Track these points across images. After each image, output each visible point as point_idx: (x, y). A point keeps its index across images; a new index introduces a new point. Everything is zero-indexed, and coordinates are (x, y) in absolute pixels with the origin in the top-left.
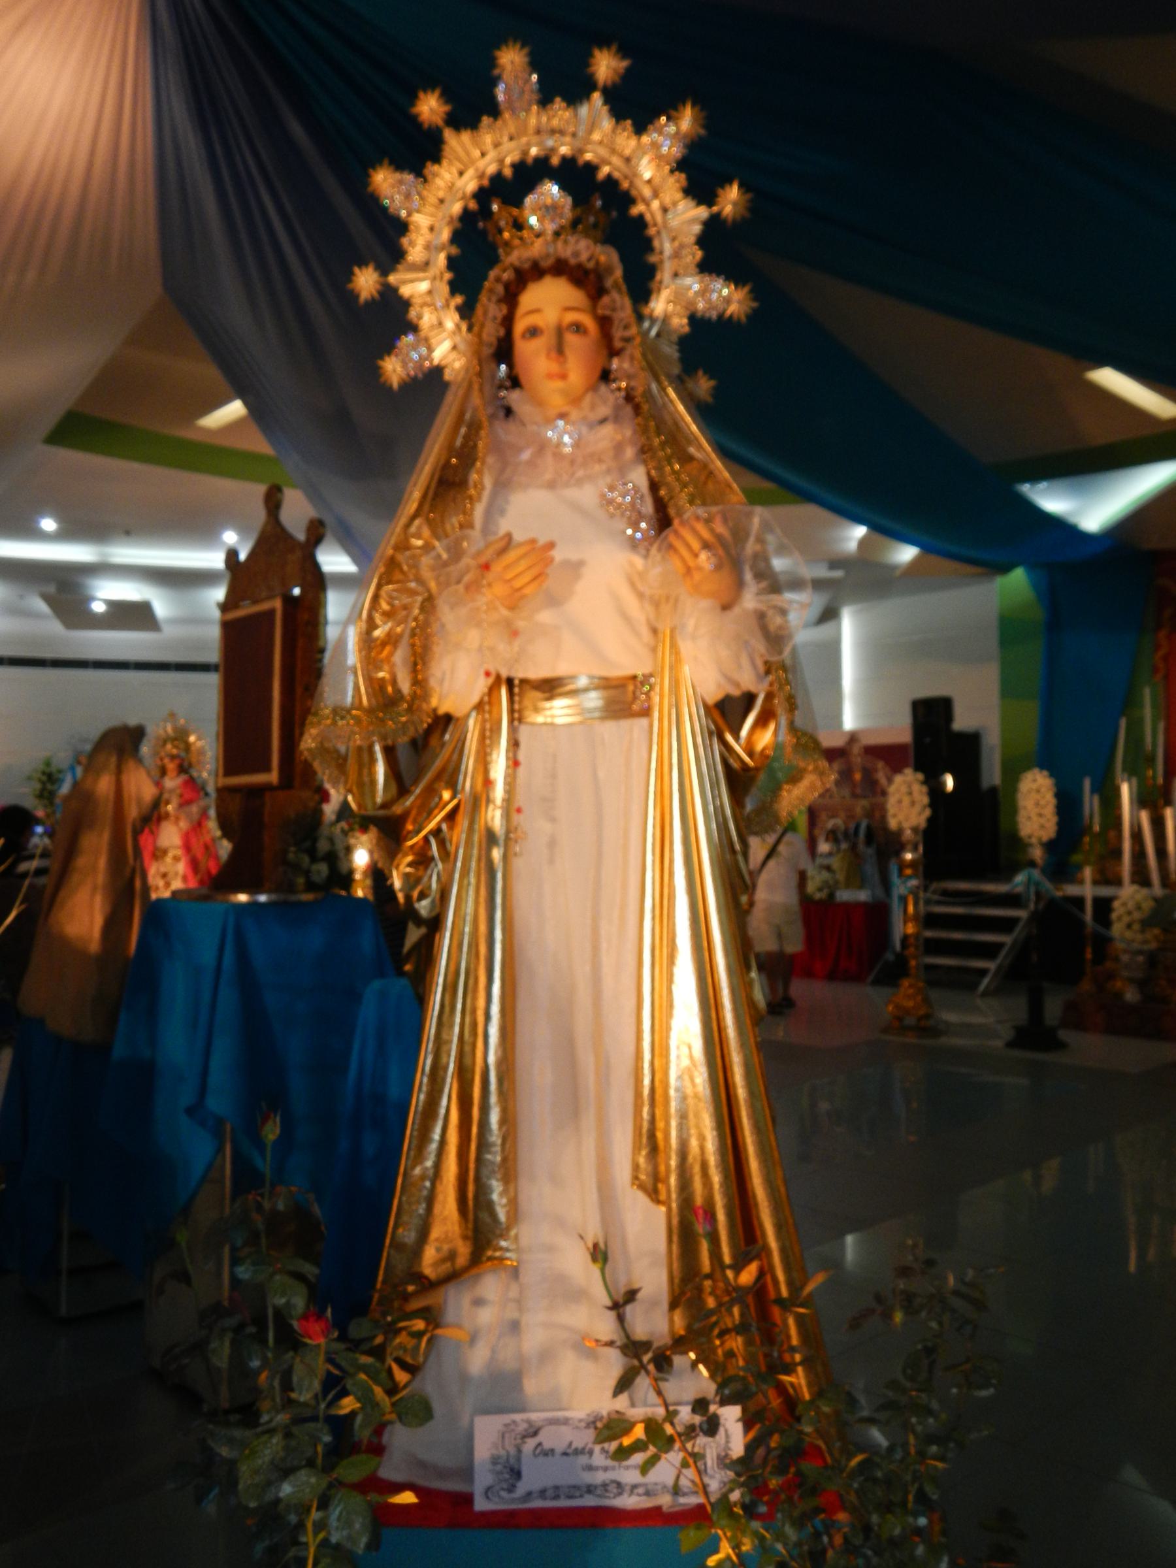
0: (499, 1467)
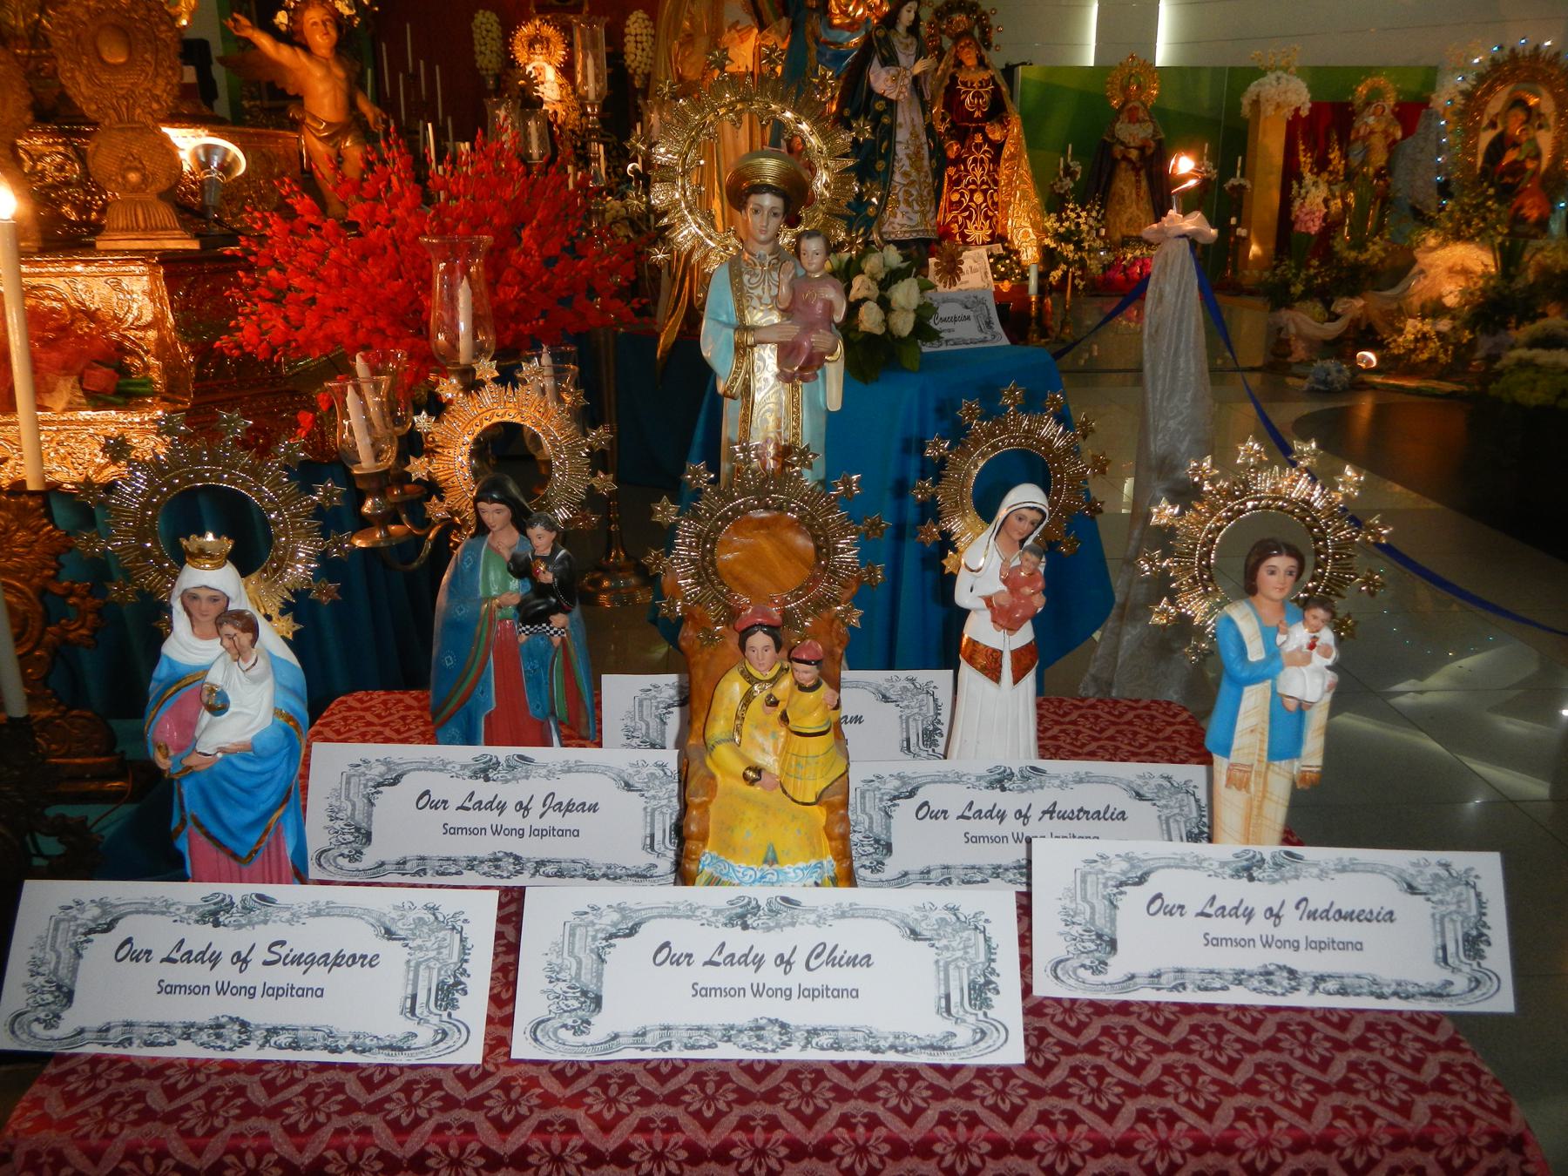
0: (560, 987)
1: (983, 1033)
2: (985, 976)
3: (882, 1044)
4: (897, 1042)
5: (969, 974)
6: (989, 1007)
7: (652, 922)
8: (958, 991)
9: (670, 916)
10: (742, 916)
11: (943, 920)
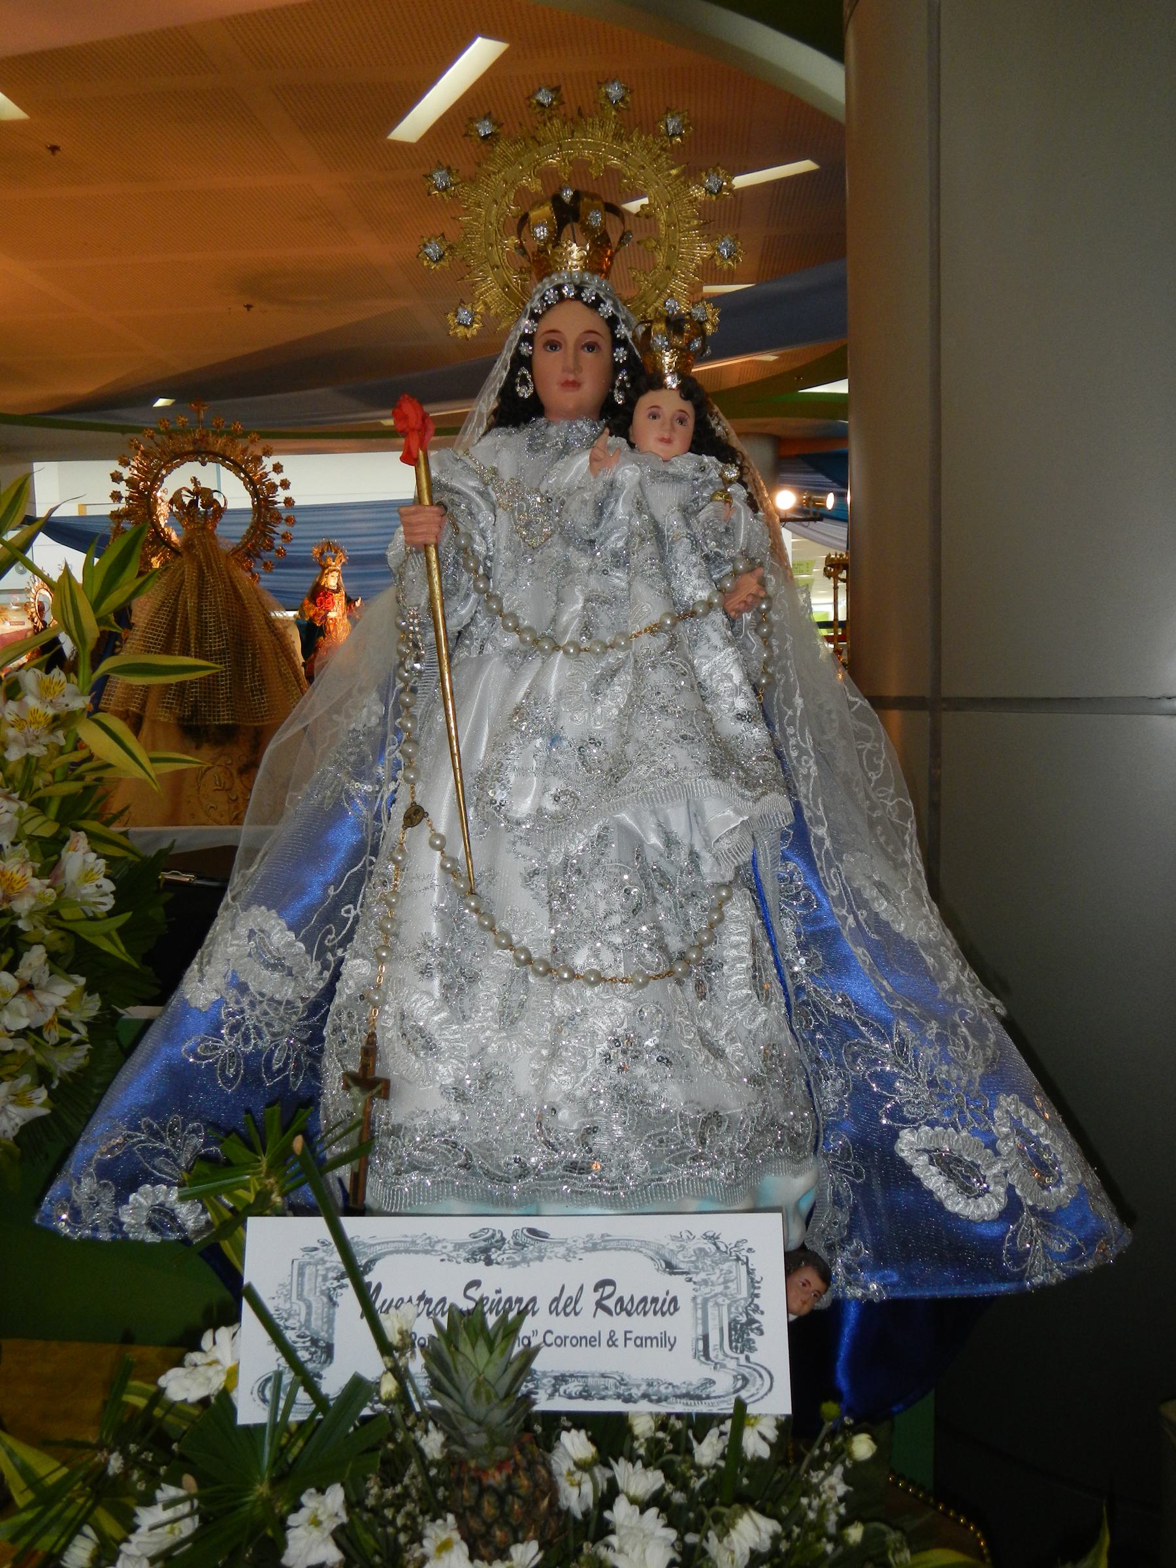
1: (745, 1380)
2: (747, 1314)
3: (636, 1393)
4: (651, 1390)
5: (729, 1312)
6: (752, 1349)
7: (388, 1258)
8: (718, 1331)
9: (407, 1251)
10: (485, 1251)
11: (701, 1250)
